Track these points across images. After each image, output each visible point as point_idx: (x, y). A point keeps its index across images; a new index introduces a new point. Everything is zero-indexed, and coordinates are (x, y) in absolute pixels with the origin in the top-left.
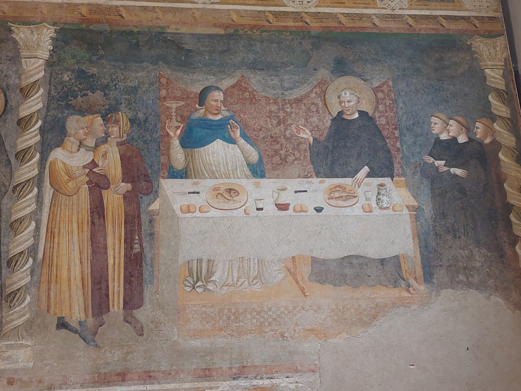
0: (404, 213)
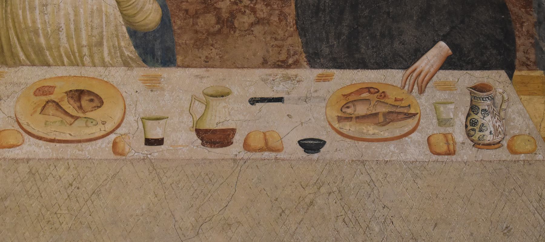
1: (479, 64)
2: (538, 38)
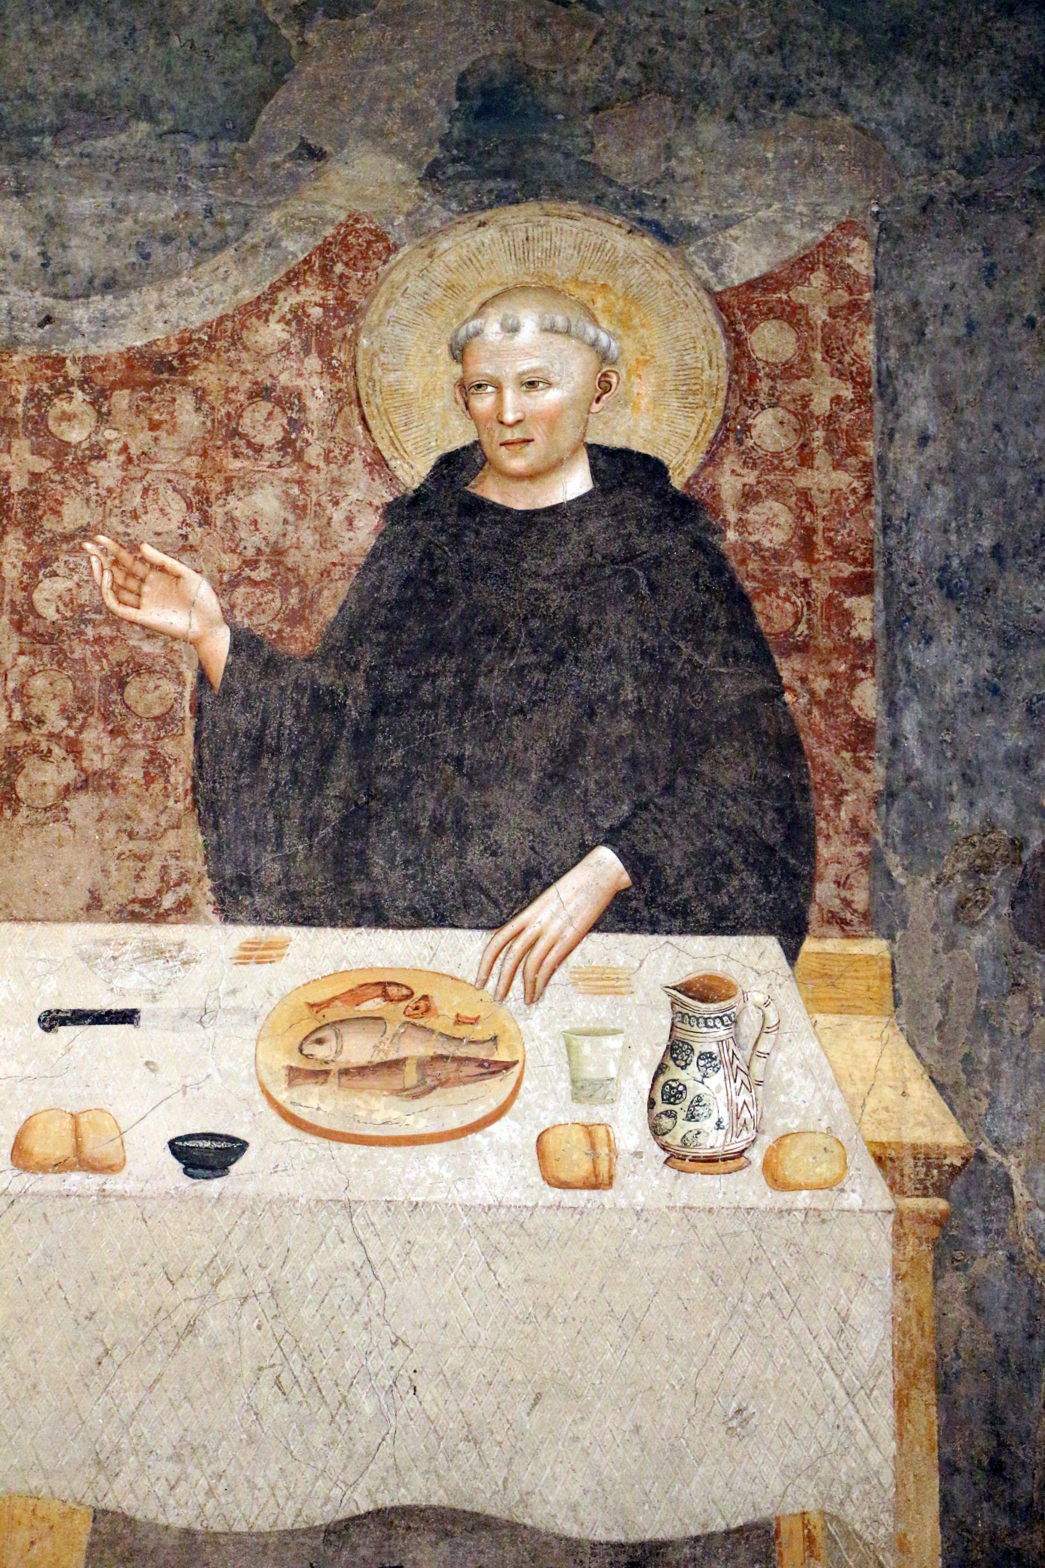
0: (853, 1200)
1: (704, 916)
2: (879, 837)
